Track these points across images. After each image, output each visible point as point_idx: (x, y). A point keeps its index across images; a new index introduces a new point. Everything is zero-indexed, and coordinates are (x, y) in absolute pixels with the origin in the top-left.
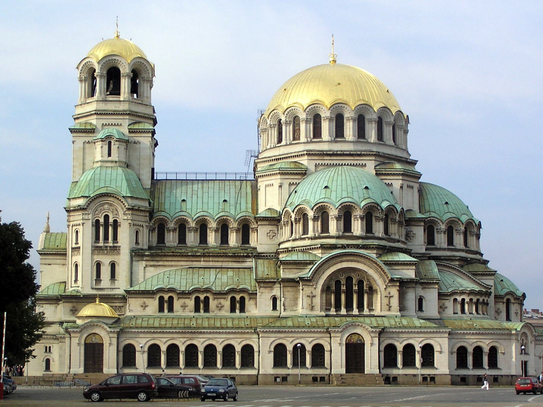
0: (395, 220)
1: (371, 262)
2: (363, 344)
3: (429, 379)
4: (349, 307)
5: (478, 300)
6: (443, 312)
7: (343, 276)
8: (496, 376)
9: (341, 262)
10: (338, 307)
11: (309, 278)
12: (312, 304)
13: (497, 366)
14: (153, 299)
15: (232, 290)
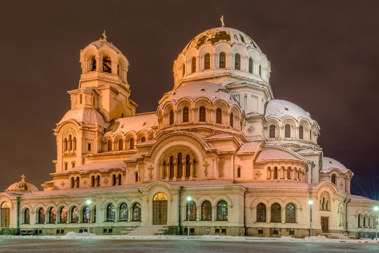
0: (227, 112)
1: (194, 140)
2: (167, 201)
3: (221, 231)
4: (179, 176)
5: (290, 168)
6: (258, 178)
7: (174, 152)
8: (292, 230)
9: (172, 141)
10: (171, 177)
11: (148, 155)
12: (151, 174)
13: (295, 220)
14: (68, 180)
15: (111, 170)
